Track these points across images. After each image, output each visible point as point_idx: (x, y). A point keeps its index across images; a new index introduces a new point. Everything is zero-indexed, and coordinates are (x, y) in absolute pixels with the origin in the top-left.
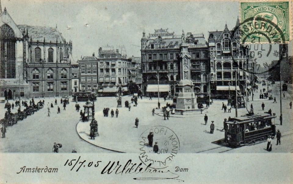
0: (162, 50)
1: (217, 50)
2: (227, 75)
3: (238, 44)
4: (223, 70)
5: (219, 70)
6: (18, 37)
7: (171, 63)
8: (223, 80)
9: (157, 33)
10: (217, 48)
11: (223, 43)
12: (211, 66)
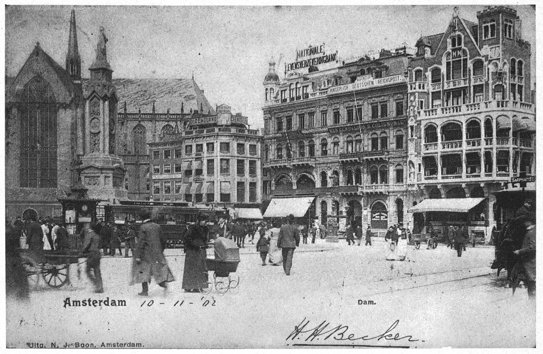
0: (290, 106)
1: (431, 90)
2: (452, 163)
3: (486, 63)
4: (439, 149)
5: (431, 150)
6: (61, 100)
7: (321, 138)
8: (464, 179)
9: (300, 60)
10: (430, 83)
11: (448, 64)
12: (410, 137)
